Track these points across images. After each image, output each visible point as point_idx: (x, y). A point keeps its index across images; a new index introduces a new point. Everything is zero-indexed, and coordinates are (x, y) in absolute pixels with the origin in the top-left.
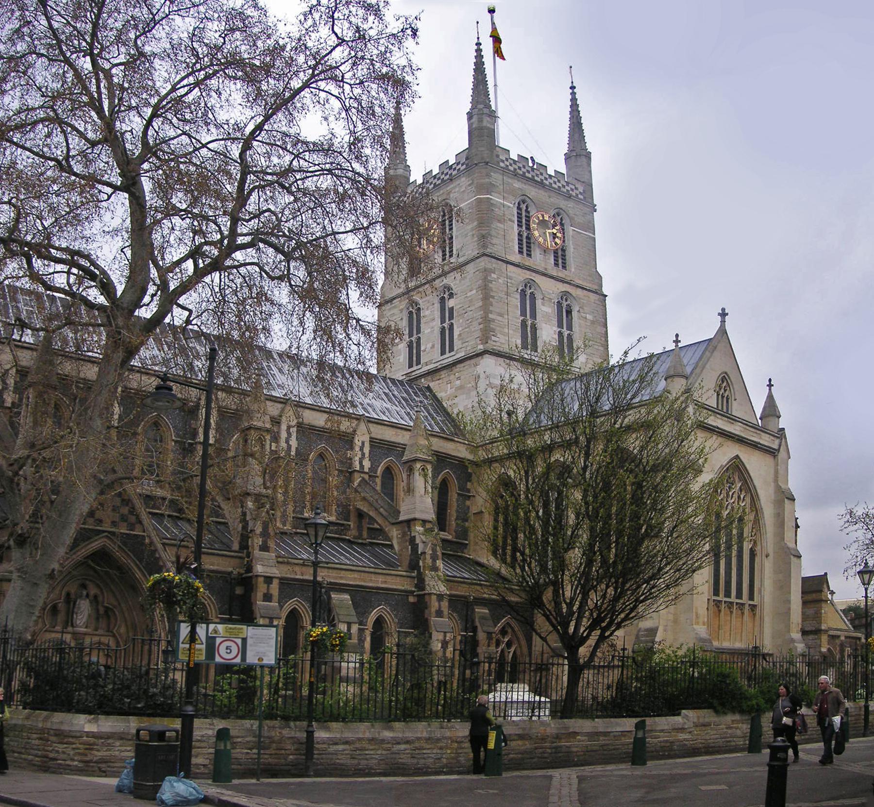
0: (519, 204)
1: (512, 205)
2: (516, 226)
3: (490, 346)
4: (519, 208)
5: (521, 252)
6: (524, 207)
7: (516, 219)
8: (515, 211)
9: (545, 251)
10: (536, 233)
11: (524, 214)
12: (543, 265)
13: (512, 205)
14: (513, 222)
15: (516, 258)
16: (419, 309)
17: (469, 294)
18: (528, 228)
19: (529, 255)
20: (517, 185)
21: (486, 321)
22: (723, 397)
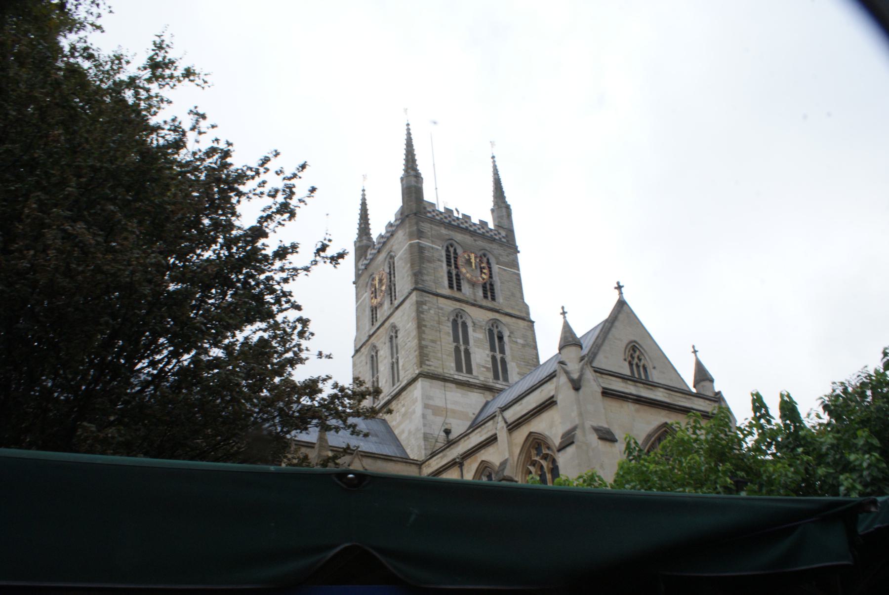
0: (447, 248)
1: (440, 248)
2: (444, 265)
3: (425, 369)
4: (448, 250)
5: (451, 286)
6: (452, 250)
7: (444, 259)
8: (444, 253)
9: (473, 284)
10: (464, 270)
11: (452, 255)
12: (473, 297)
13: (440, 248)
14: (442, 261)
15: (446, 291)
16: (377, 353)
17: (407, 328)
18: (457, 267)
19: (459, 289)
20: (444, 231)
21: (421, 348)
22: (638, 366)
